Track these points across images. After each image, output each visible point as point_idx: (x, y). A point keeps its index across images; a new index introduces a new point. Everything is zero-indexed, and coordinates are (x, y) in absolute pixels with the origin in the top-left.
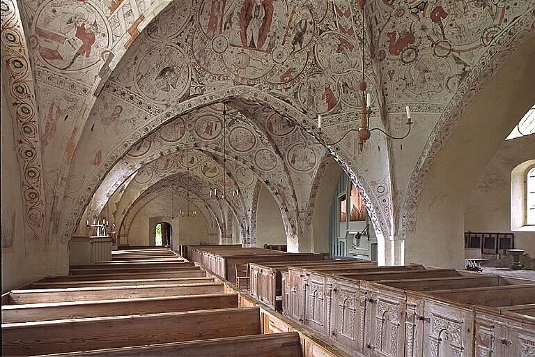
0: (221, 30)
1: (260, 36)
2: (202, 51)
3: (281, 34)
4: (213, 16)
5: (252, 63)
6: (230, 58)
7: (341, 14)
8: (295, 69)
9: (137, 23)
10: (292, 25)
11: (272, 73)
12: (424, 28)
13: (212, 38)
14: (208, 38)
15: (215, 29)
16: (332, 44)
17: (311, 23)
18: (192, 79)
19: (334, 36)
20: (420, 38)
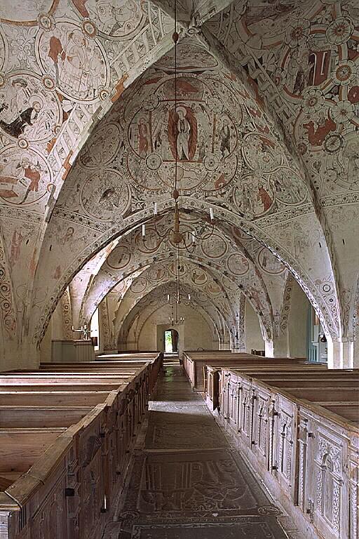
0: (152, 149)
2: (137, 170)
3: (209, 143)
4: (142, 138)
6: (166, 172)
8: (227, 174)
9: (68, 158)
11: (205, 181)
12: (343, 113)
14: (142, 158)
17: (232, 127)
18: (133, 197)
20: (341, 123)
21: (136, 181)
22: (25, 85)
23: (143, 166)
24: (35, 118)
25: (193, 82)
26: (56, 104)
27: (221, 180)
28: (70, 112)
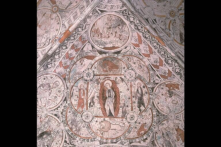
0: (87, 107)
1: (115, 108)
2: (74, 121)
4: (80, 98)
5: (113, 127)
6: (95, 126)
7: (157, 67)
8: (145, 123)
10: (133, 95)
11: (129, 132)
15: (83, 107)
16: (164, 93)
17: (144, 87)
18: (65, 141)
21: (71, 129)
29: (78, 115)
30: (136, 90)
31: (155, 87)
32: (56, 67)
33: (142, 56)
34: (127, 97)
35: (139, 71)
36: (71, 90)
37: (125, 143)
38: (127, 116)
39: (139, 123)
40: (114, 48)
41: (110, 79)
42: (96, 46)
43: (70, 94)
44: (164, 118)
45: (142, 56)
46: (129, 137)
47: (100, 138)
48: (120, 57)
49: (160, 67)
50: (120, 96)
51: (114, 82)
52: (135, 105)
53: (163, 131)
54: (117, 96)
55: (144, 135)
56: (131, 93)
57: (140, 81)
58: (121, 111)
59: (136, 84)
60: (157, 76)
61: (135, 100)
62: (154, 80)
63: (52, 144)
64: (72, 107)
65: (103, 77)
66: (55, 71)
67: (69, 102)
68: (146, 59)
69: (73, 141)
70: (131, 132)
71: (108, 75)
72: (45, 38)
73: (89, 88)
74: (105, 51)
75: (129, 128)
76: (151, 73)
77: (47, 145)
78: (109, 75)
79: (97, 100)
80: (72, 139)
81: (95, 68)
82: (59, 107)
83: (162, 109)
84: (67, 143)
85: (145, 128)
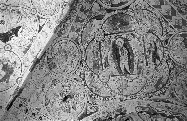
1: (129, 65)
2: (92, 82)
3: (143, 58)
5: (130, 84)
8: (163, 77)
10: (147, 50)
13: (98, 74)
14: (95, 74)
15: (98, 68)
17: (157, 40)
19: (176, 37)
21: (91, 90)
22: (19, 12)
23: (96, 79)
24: (21, 32)
25: (124, 18)
26: (36, 23)
27: (159, 82)
28: (43, 25)
29: (95, 76)
30: (149, 45)
31: (169, 38)
32: (68, 32)
33: (152, 8)
34: (141, 52)
35: (151, 25)
36: (85, 54)
37: (144, 98)
38: (142, 72)
39: (156, 77)
40: (121, 4)
41: (122, 37)
42: (103, 5)
43: (85, 57)
44: (181, 69)
45: (152, 8)
46: (148, 92)
47: (119, 96)
48: (129, 13)
49: (173, 17)
50: (133, 53)
51: (126, 40)
52: (150, 60)
53: (182, 82)
54: (131, 53)
55: (162, 88)
56: (145, 48)
57: (153, 35)
58: (136, 67)
59: (149, 39)
60: (171, 27)
61: (149, 55)
62: (167, 32)
63: (77, 106)
64: (89, 69)
65: (115, 35)
66: (68, 37)
67: (84, 65)
68: (156, 11)
69: (94, 101)
70: (149, 86)
71: (118, 33)
72: (55, 4)
73: (102, 49)
74: (113, 9)
75: (146, 83)
76: (163, 25)
77: (72, 107)
78: (120, 33)
79: (111, 59)
80: (93, 99)
81: (105, 28)
82: (77, 71)
83: (179, 61)
84: (89, 104)
85: (163, 82)
